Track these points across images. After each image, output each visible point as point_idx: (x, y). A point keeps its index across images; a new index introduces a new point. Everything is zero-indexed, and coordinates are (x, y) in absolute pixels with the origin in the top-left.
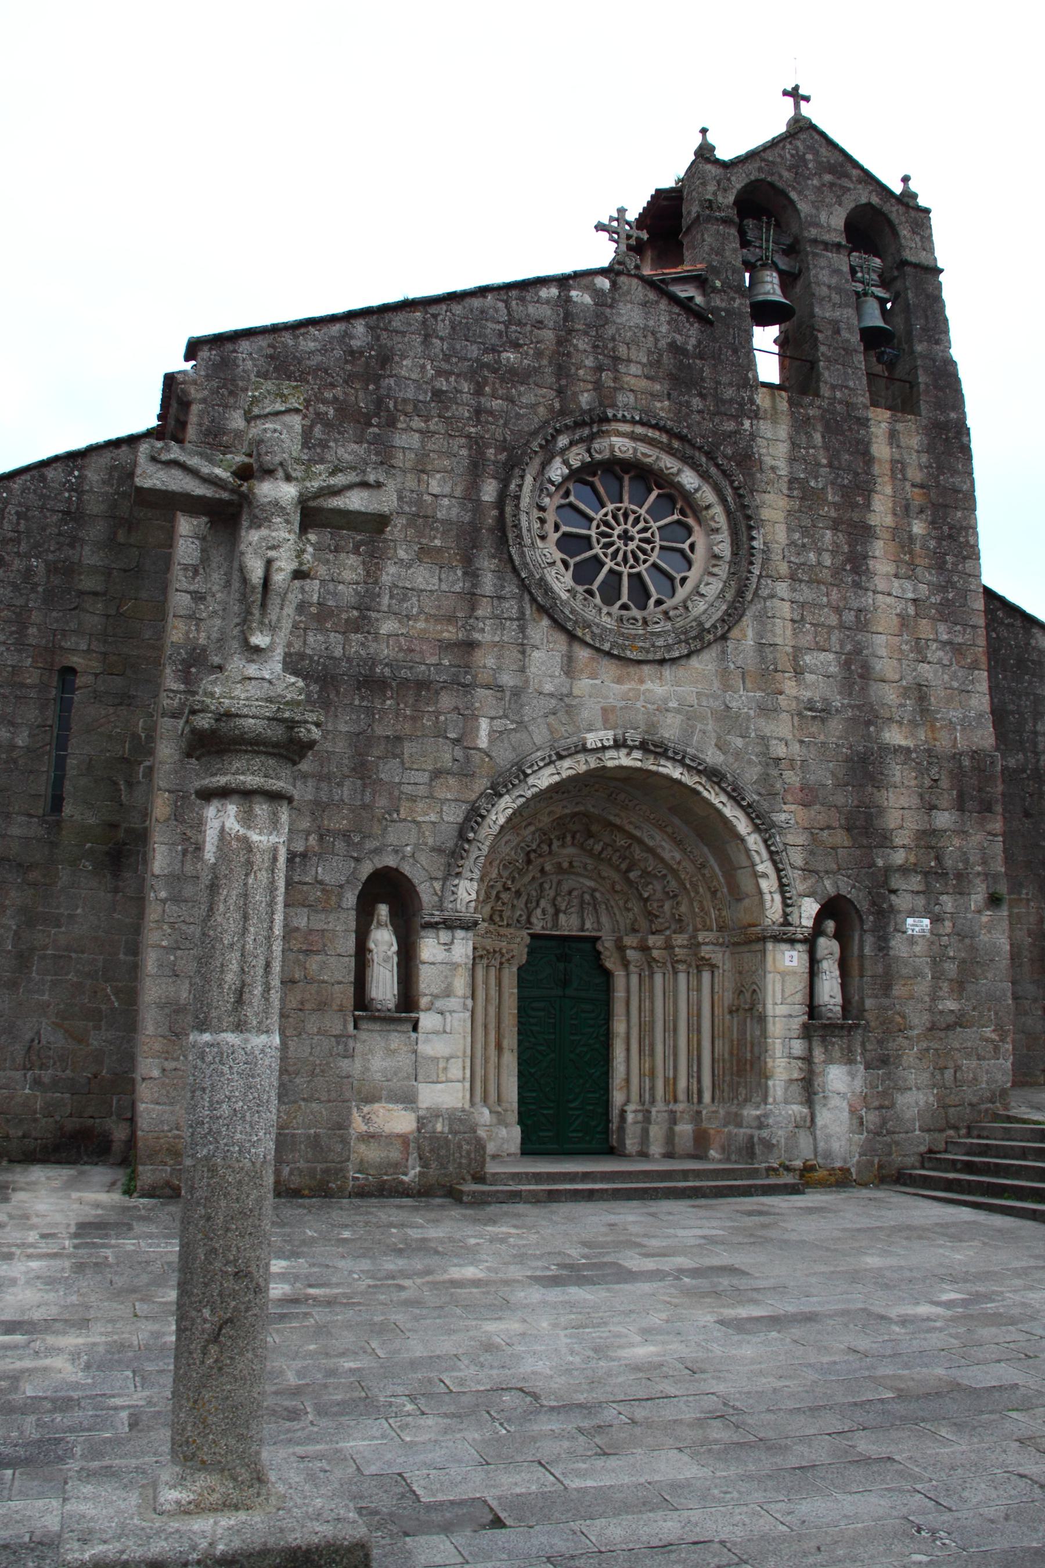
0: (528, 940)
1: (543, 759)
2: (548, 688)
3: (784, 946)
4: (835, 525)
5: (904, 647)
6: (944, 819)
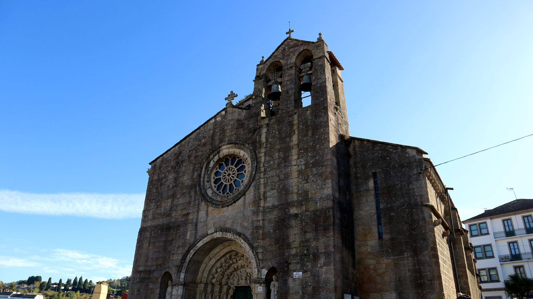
0: (234, 288)
2: (202, 220)
3: (258, 285)
4: (279, 150)
5: (300, 180)
6: (309, 236)
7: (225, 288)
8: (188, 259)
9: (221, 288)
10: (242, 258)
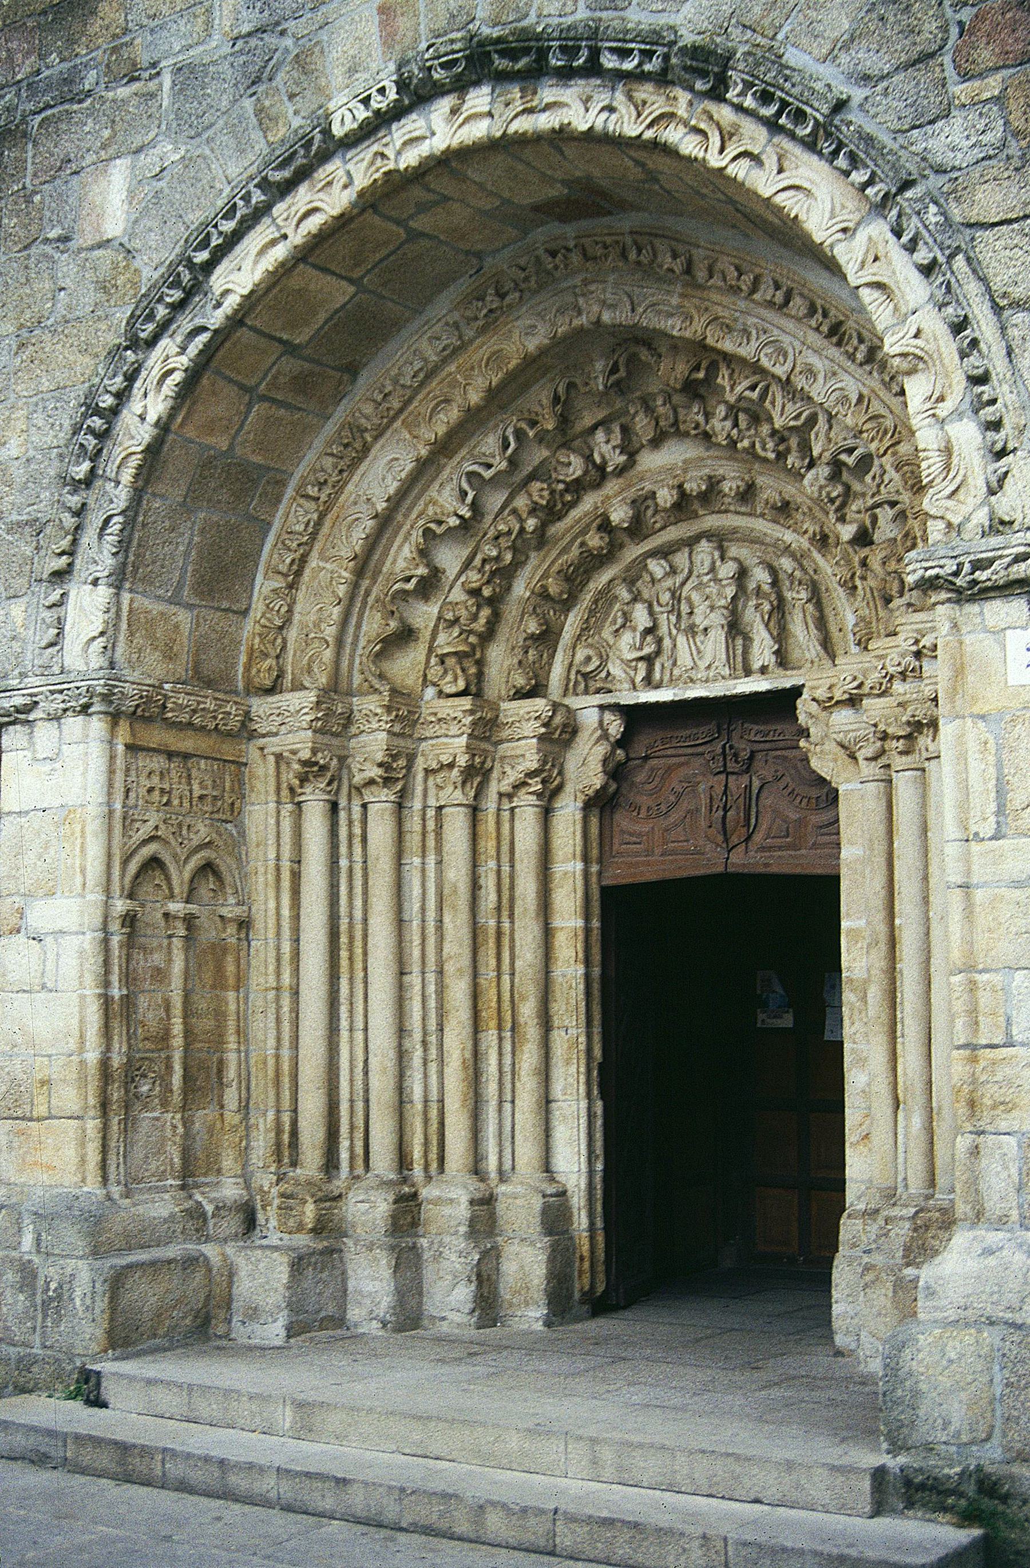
0: (615, 727)
1: (230, 213)
7: (524, 718)
8: (135, 431)
9: (486, 730)
10: (695, 414)
